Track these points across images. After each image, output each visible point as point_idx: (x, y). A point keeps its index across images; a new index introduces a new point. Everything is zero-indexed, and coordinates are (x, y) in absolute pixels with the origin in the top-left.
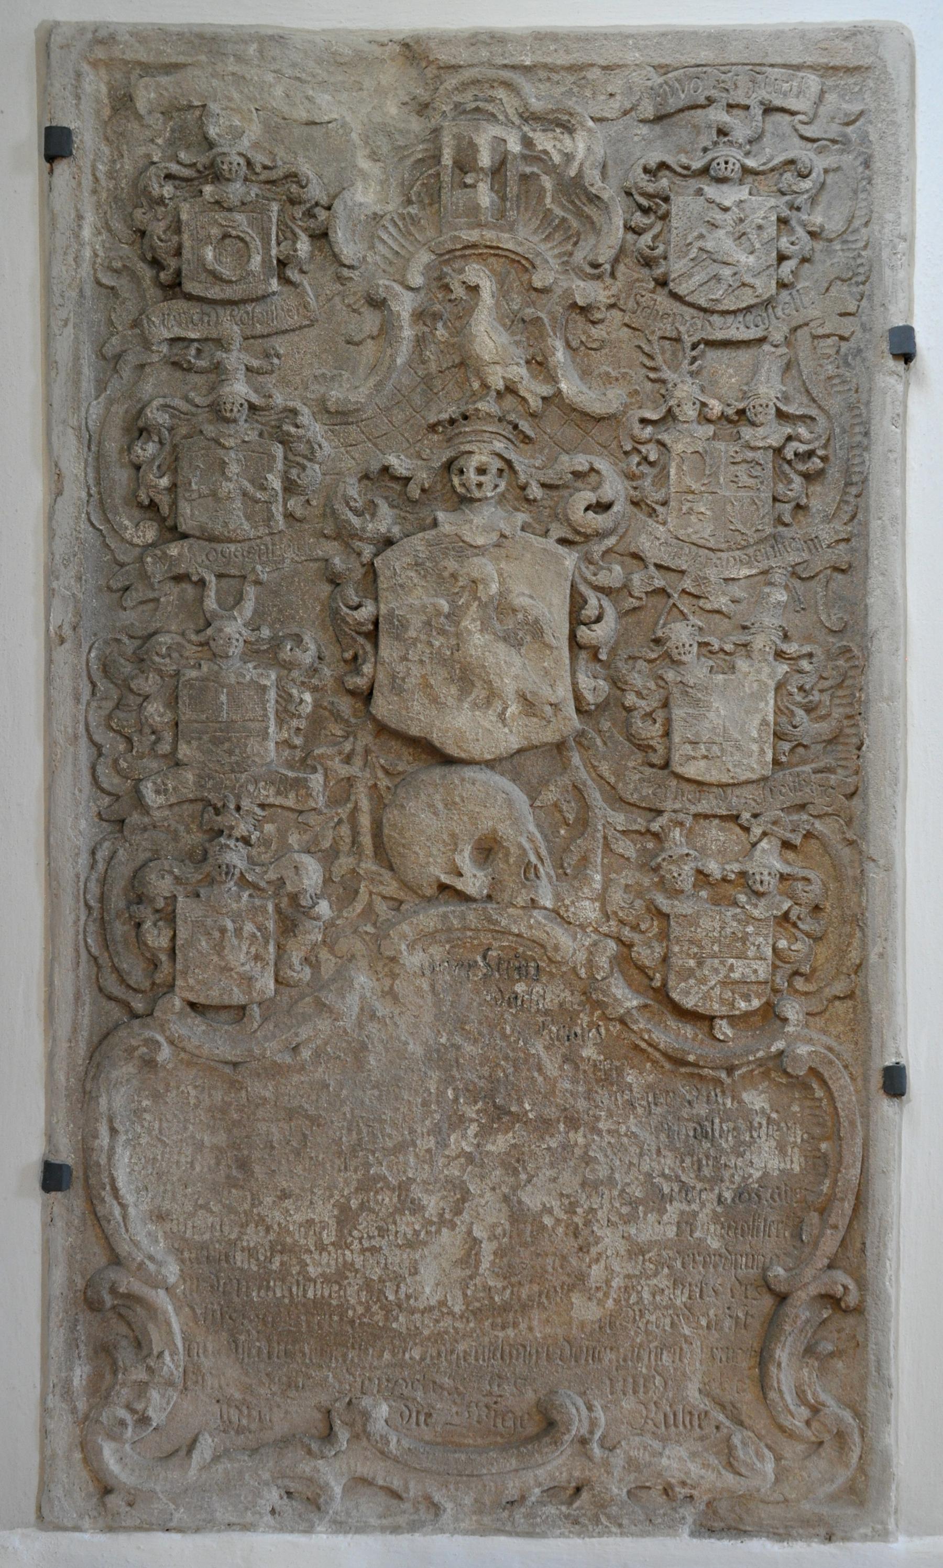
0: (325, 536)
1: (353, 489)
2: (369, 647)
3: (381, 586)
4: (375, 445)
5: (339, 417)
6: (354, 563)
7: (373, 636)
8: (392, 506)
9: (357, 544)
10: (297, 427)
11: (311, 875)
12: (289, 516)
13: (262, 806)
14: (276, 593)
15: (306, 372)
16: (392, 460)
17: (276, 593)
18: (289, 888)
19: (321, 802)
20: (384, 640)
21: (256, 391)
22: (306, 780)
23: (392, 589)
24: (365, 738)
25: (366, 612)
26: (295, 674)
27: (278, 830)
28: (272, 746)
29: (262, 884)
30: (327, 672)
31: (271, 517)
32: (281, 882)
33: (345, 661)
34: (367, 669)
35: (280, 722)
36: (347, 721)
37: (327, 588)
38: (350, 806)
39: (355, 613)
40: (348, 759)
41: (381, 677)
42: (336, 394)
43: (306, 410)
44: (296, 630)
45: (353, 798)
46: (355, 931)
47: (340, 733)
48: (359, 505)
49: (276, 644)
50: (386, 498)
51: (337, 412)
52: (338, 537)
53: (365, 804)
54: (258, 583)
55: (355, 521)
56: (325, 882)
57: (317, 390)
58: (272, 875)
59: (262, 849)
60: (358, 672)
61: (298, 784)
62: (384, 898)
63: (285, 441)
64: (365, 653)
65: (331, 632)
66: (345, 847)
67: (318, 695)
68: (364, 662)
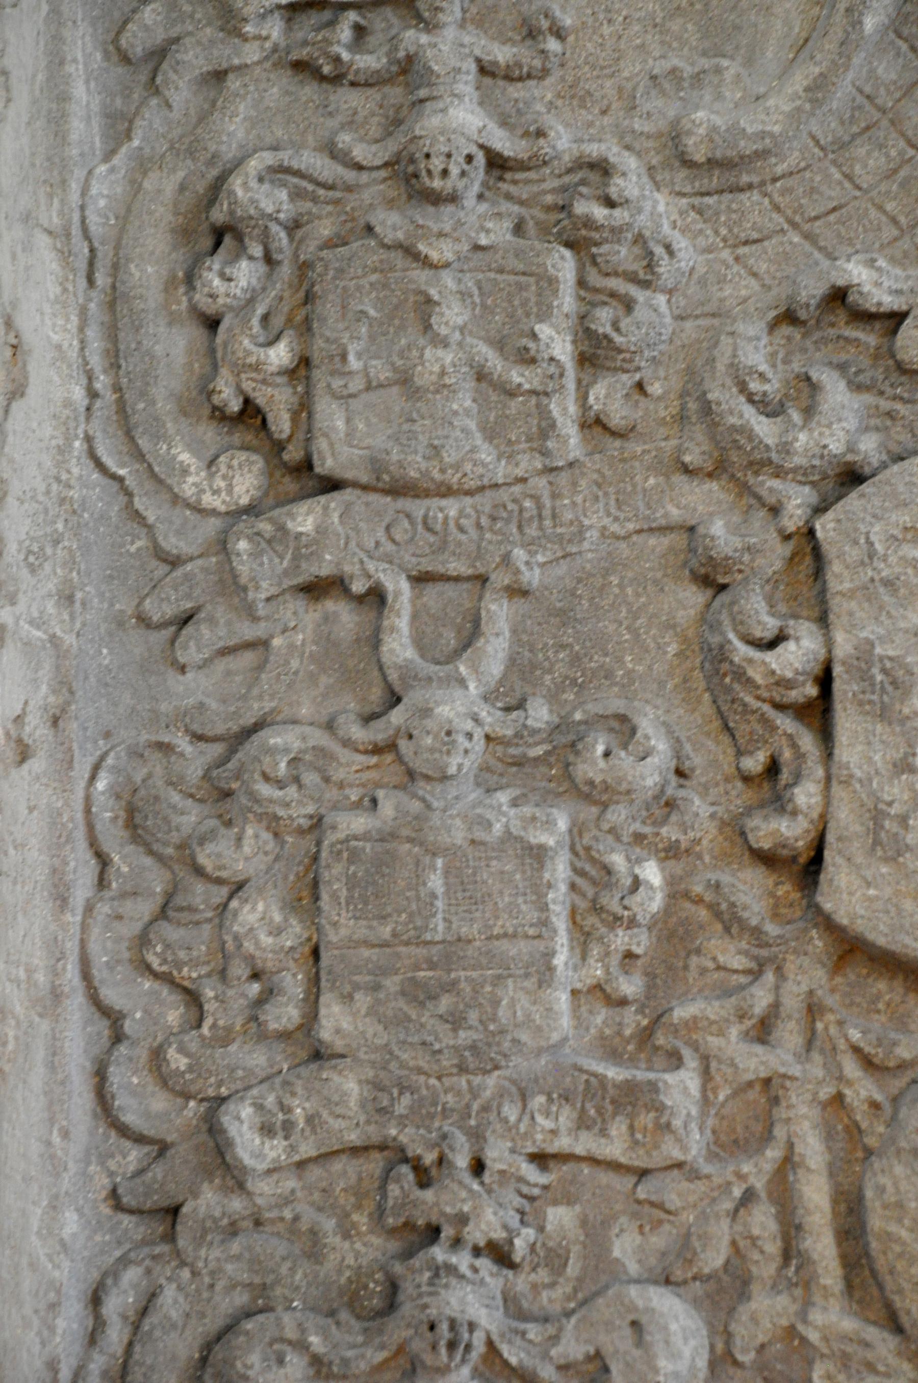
0: (686, 470)
1: (755, 350)
2: (808, 742)
3: (834, 585)
4: (807, 236)
5: (716, 173)
7: (819, 711)
8: (857, 387)
9: (769, 485)
10: (610, 204)
12: (594, 424)
13: (540, 1159)
14: (564, 616)
15: (630, 68)
16: (856, 272)
17: (564, 616)
19: (695, 1145)
20: (847, 722)
21: (504, 123)
22: (653, 1087)
23: (866, 591)
24: (807, 973)
25: (798, 654)
26: (618, 815)
27: (584, 1222)
28: (563, 999)
30: (699, 806)
31: (547, 428)
33: (747, 779)
34: (807, 796)
35: (583, 938)
36: (757, 932)
37: (693, 598)
39: (770, 658)
40: (763, 1031)
41: (846, 818)
42: (707, 120)
43: (631, 162)
44: (617, 705)
45: (780, 1132)
47: (738, 962)
48: (772, 388)
49: (567, 741)
50: (842, 368)
51: (712, 163)
52: (718, 469)
53: (813, 1149)
54: (517, 592)
55: (765, 429)
57: (658, 110)
58: (572, 1347)
59: (543, 1276)
60: (780, 803)
61: (633, 1098)
63: (580, 241)
64: (800, 756)
65: (706, 706)
67: (677, 867)
68: (797, 778)
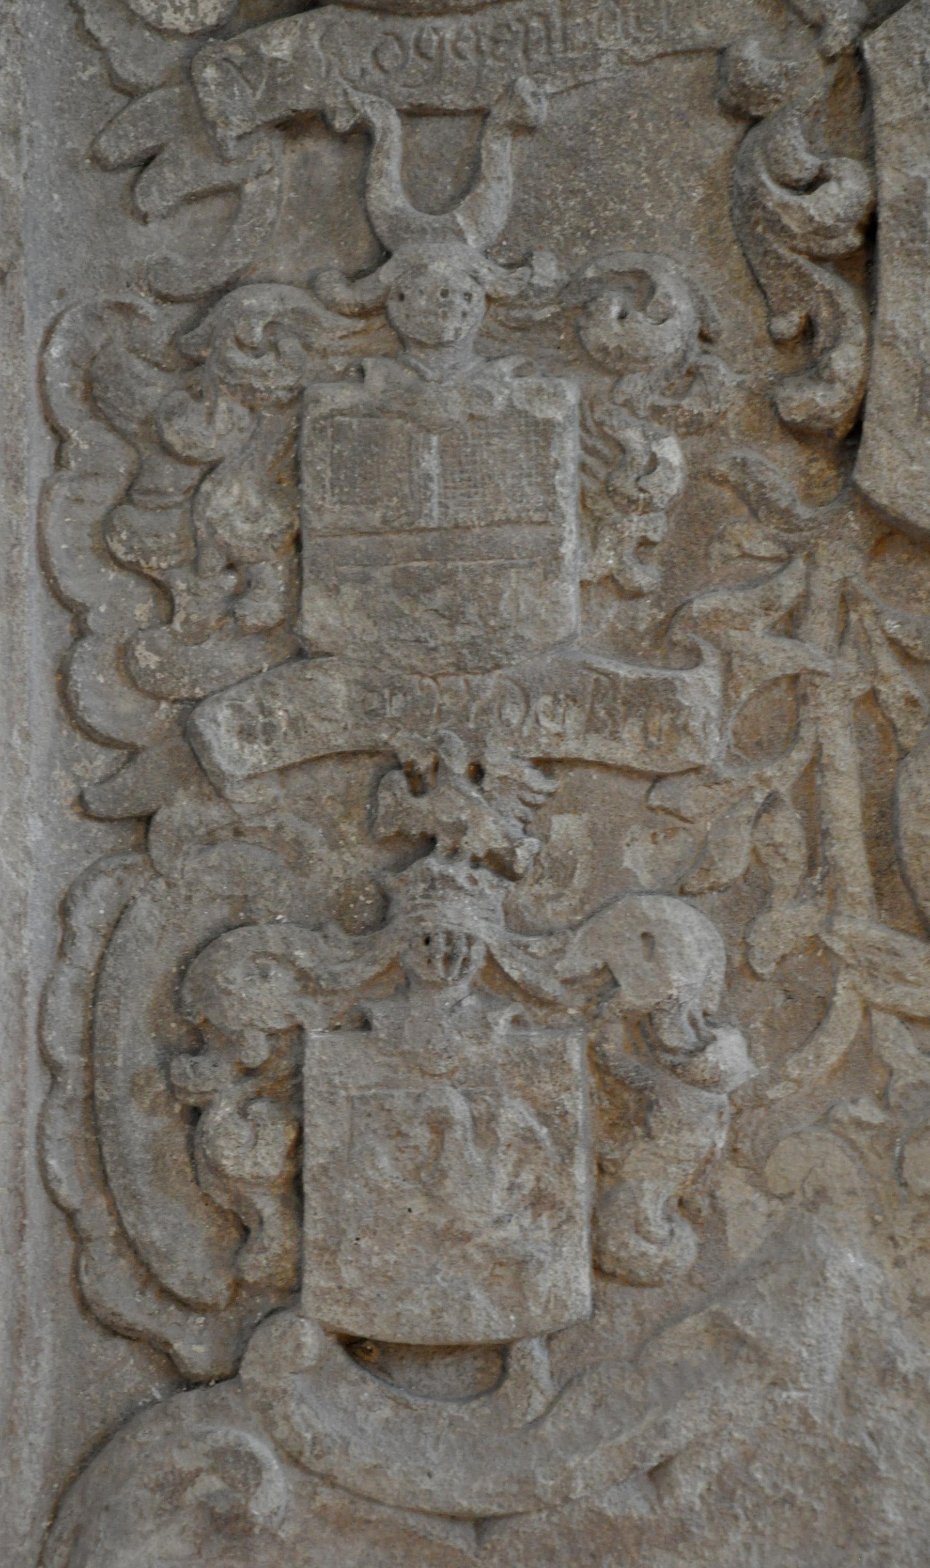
2: (848, 299)
3: (883, 115)
6: (803, 56)
7: (861, 264)
11: (693, 955)
13: (545, 765)
14: (575, 156)
18: (630, 996)
19: (714, 747)
20: (893, 275)
24: (841, 560)
27: (592, 832)
28: (571, 592)
29: (551, 988)
30: (725, 375)
32: (607, 978)
33: (779, 343)
34: (845, 360)
35: (594, 525)
36: (786, 514)
37: (722, 133)
38: (800, 755)
39: (807, 201)
40: (791, 624)
41: (889, 385)
44: (634, 260)
45: (807, 732)
46: (825, 1119)
47: (765, 549)
49: (577, 300)
53: (843, 750)
54: (522, 128)
56: (730, 978)
58: (579, 960)
59: (547, 887)
60: (816, 371)
62: (908, 1019)
64: (839, 315)
65: (735, 262)
66: (787, 875)
67: (699, 444)
68: (836, 340)
